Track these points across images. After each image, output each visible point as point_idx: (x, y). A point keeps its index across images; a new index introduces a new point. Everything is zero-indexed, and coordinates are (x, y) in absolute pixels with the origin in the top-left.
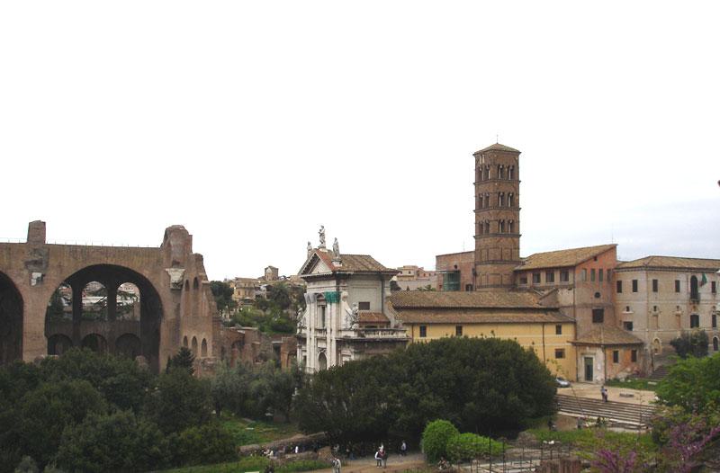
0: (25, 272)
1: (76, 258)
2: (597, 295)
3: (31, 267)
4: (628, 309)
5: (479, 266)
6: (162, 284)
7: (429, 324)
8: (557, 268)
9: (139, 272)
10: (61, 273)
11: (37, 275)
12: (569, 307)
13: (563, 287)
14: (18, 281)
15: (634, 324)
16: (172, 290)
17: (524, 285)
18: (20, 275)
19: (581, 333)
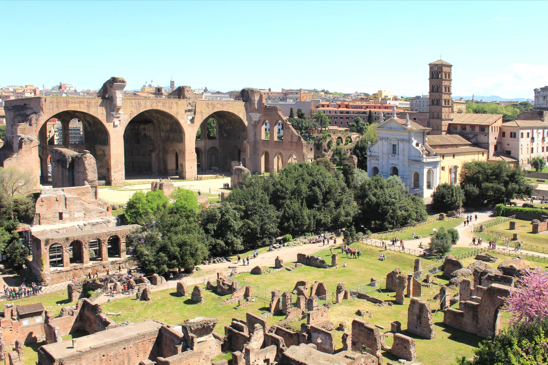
0: (185, 116)
1: (209, 108)
4: (508, 145)
11: (190, 118)
12: (485, 143)
14: (182, 122)
15: (512, 152)
18: (183, 118)
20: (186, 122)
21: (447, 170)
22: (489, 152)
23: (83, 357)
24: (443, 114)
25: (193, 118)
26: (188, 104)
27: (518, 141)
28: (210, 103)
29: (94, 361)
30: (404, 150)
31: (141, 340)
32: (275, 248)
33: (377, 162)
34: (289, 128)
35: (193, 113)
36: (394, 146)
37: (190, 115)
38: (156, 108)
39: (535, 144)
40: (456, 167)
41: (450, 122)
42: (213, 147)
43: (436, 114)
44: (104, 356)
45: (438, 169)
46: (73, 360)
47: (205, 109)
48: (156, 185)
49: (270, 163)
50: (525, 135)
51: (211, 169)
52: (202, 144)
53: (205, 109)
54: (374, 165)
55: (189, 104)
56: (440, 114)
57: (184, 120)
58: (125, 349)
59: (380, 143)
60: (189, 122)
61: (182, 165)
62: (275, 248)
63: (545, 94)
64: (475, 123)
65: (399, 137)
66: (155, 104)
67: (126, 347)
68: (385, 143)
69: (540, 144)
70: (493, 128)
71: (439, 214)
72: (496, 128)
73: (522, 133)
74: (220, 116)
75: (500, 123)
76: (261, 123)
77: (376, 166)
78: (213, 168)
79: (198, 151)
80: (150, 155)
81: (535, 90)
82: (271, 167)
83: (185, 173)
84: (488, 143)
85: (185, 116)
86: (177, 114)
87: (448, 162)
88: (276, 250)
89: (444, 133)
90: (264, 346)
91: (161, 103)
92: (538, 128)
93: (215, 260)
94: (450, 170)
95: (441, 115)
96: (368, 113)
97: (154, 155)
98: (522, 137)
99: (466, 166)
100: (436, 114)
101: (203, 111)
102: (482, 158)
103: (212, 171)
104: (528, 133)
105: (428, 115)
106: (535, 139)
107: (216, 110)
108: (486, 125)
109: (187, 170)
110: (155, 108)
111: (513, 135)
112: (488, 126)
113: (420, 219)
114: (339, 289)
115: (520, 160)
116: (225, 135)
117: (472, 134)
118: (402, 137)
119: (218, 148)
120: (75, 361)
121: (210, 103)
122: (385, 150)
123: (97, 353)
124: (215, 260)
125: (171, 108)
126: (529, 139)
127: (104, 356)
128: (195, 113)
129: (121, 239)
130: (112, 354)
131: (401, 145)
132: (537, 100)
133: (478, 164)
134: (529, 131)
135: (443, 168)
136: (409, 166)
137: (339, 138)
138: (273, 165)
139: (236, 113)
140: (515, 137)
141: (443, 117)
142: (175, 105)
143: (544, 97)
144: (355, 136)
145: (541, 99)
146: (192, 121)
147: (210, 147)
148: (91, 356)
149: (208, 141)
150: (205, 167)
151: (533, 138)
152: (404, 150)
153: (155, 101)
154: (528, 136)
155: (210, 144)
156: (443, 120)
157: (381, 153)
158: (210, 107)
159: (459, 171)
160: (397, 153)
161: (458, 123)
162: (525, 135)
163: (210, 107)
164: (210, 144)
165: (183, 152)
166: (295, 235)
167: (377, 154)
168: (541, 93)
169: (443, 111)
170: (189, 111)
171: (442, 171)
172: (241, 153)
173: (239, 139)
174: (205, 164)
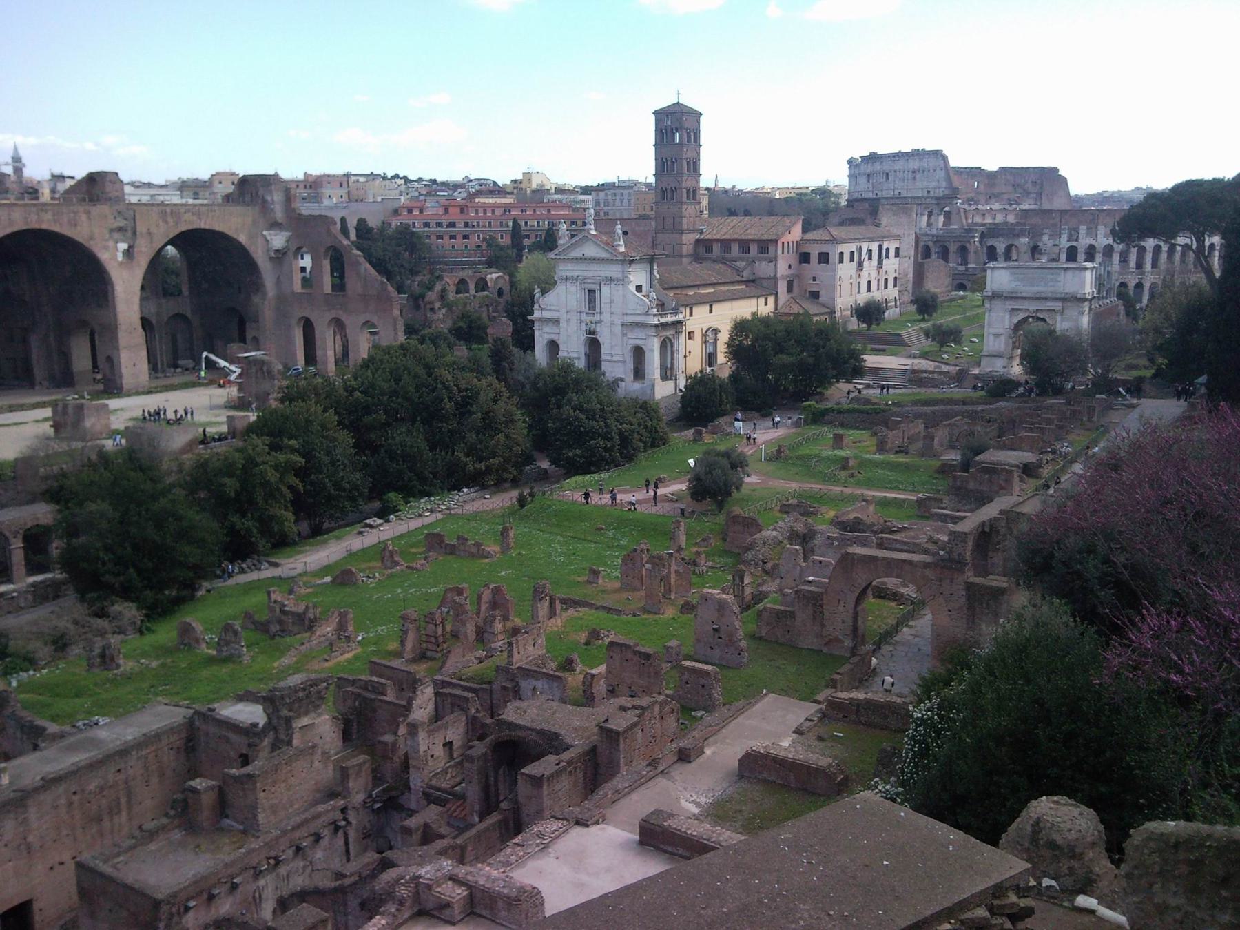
0: (111, 244)
1: (166, 222)
2: (790, 266)
3: (116, 235)
4: (814, 279)
5: (659, 235)
6: (260, 252)
7: (696, 304)
8: (753, 241)
9: (235, 237)
10: (151, 243)
11: (123, 246)
13: (760, 260)
14: (104, 256)
16: (271, 258)
17: (709, 255)
18: (106, 248)
19: (780, 303)
20: (114, 257)
21: (698, 336)
22: (776, 295)
23: (30, 802)
24: (685, 221)
25: (130, 247)
26: (116, 214)
27: (834, 270)
28: (168, 210)
29: (56, 807)
30: (612, 302)
31: (153, 748)
32: (371, 527)
33: (555, 330)
34: (358, 263)
35: (129, 234)
36: (591, 293)
37: (123, 241)
38: (37, 226)
39: (864, 273)
40: (716, 331)
41: (698, 236)
42: (177, 315)
43: (669, 222)
44: (75, 793)
45: (682, 337)
46: (9, 812)
47: (157, 226)
48: (65, 407)
49: (318, 343)
50: (847, 257)
51: (176, 366)
52: (152, 309)
53: (157, 226)
54: (548, 337)
55: (119, 213)
56: (677, 220)
57: (112, 254)
58: (119, 771)
59: (560, 289)
60: (120, 257)
61: (110, 360)
62: (371, 527)
63: (869, 169)
64: (750, 237)
65: (603, 274)
66: (34, 217)
67: (122, 766)
68: (573, 289)
69: (874, 274)
70: (786, 245)
71: (692, 431)
72: (791, 244)
73: (841, 254)
74: (189, 241)
75: (797, 232)
76: (290, 254)
77: (553, 337)
78: (180, 362)
79: (146, 323)
80: (25, 341)
81: (850, 162)
82: (319, 353)
83: (121, 377)
84: (775, 278)
85: (111, 244)
86: (91, 238)
87: (699, 319)
88: (375, 531)
89: (685, 260)
90: (437, 716)
91: (50, 213)
92: (871, 239)
93: (244, 566)
94: (705, 335)
95: (681, 223)
96: (511, 223)
97: (34, 342)
98: (841, 261)
99: (740, 327)
100: (669, 222)
101: (154, 230)
102: (765, 308)
103: (179, 370)
104: (852, 253)
105: (653, 223)
106: (866, 264)
107: (184, 228)
108: (771, 241)
109: (124, 371)
110: (35, 225)
111: (824, 258)
112: (776, 241)
113: (656, 441)
114: (538, 594)
115: (837, 308)
116: (205, 285)
117: (743, 261)
118: (609, 275)
119: (189, 314)
120: (12, 816)
121: (168, 210)
122: (573, 303)
123: (61, 789)
124: (244, 566)
125: (76, 225)
126: (855, 264)
127: (75, 793)
128: (134, 233)
129: (13, 540)
130: (92, 786)
131: (605, 290)
132: (854, 183)
133: (765, 321)
134: (853, 247)
135: (691, 335)
136: (624, 335)
137: (462, 282)
138: (325, 349)
139: (230, 233)
140: (827, 262)
141: (685, 227)
142: (84, 217)
143: (869, 175)
144: (494, 276)
145: (862, 180)
146: (129, 253)
147: (171, 313)
148: (47, 797)
149: (163, 301)
150: (162, 365)
151: (860, 264)
152: (612, 302)
153: (34, 209)
154: (852, 260)
155: (170, 307)
156: (681, 232)
157: (563, 311)
158: (170, 220)
159: (724, 337)
160: (598, 310)
161: (715, 237)
162: (847, 257)
163: (170, 220)
164: (170, 307)
165: (111, 329)
166: (410, 493)
167: (554, 315)
168: (863, 168)
169: (684, 213)
170: (120, 229)
171: (689, 342)
172: (248, 325)
173: (240, 292)
174: (161, 355)
